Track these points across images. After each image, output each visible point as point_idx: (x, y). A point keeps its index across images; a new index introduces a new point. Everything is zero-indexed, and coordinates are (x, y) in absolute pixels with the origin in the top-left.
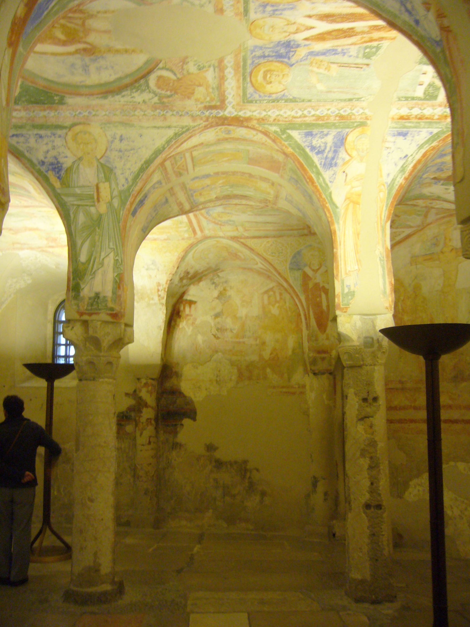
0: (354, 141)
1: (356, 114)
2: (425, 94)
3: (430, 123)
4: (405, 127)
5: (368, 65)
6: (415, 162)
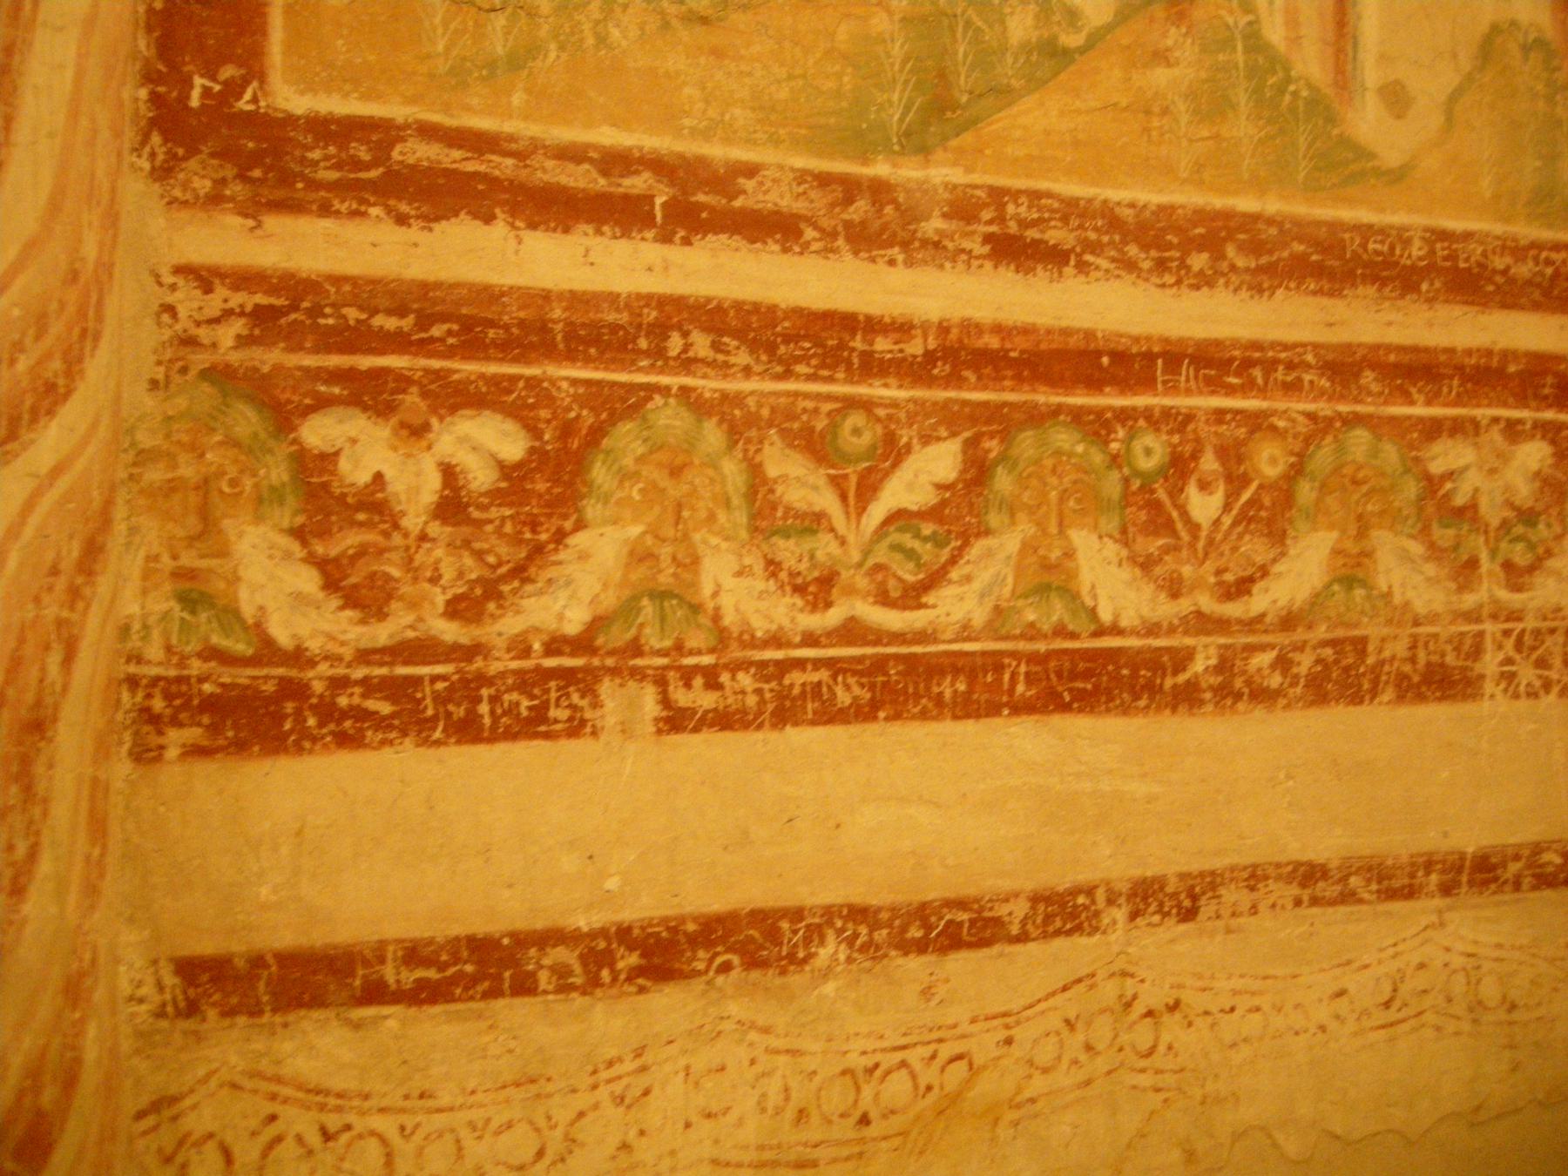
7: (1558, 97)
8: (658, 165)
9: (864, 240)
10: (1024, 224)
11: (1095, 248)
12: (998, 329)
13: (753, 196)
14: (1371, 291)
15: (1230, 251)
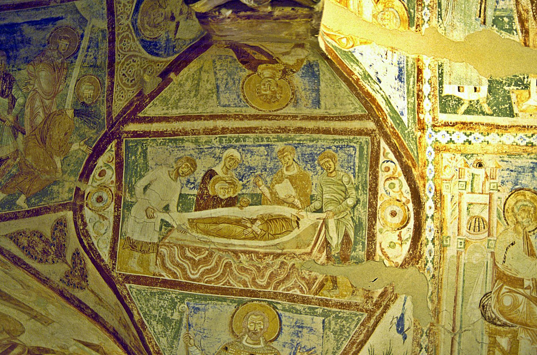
0: (393, 8)
1: (423, 12)
2: (448, 96)
3: (414, 110)
4: (408, 78)
5: (484, 23)
6: (373, 93)
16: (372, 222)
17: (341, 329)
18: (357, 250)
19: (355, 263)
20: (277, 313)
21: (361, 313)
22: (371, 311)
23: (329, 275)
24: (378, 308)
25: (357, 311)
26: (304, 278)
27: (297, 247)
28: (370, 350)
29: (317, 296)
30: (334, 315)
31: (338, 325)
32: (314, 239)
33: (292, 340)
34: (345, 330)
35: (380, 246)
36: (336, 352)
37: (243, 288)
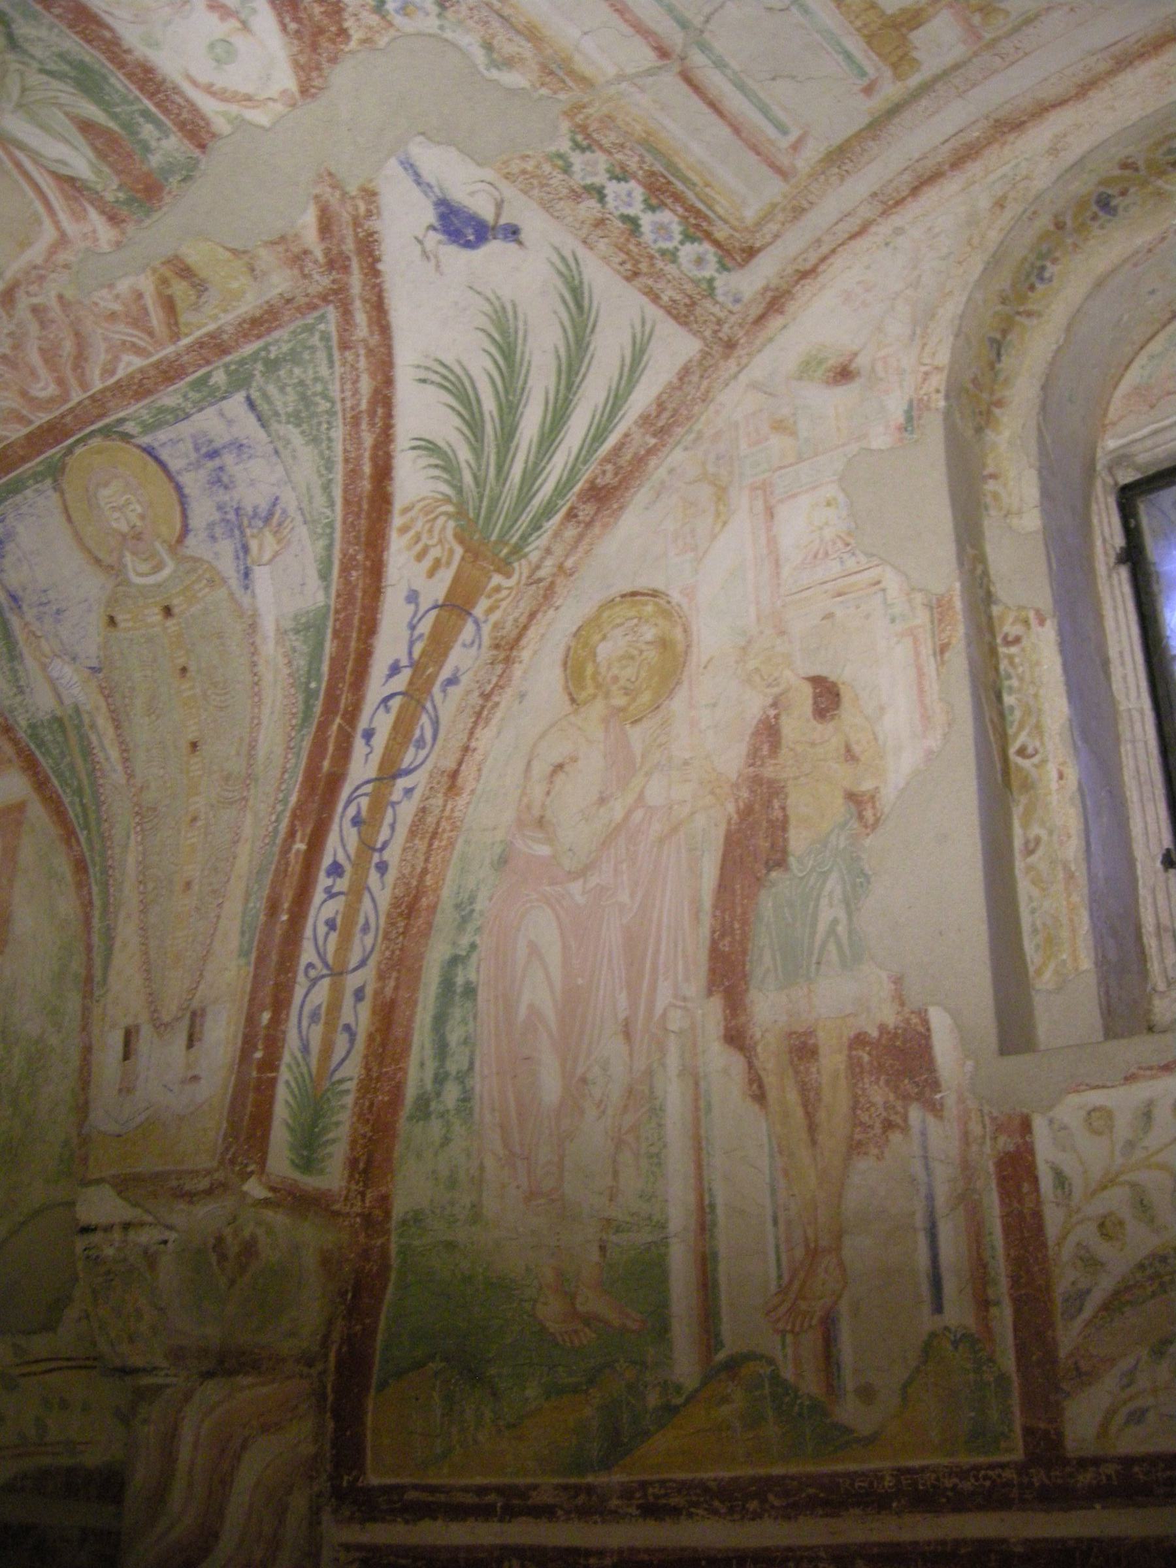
7: (984, 1368)
8: (500, 1490)
9: (584, 1513)
10: (657, 1497)
11: (696, 1505)
12: (647, 1551)
13: (536, 1499)
14: (857, 1511)
15: (771, 1497)
16: (103, 39)
17: (303, 397)
18: (153, 144)
19: (184, 180)
20: (139, 446)
21: (316, 314)
22: (335, 292)
23: (157, 263)
24: (346, 269)
25: (303, 314)
26: (113, 316)
27: (24, 245)
28: (423, 374)
29: (185, 341)
30: (260, 366)
31: (289, 389)
32: (31, 194)
33: (220, 508)
34: (315, 394)
35: (195, 83)
36: (330, 481)
37: (26, 431)
